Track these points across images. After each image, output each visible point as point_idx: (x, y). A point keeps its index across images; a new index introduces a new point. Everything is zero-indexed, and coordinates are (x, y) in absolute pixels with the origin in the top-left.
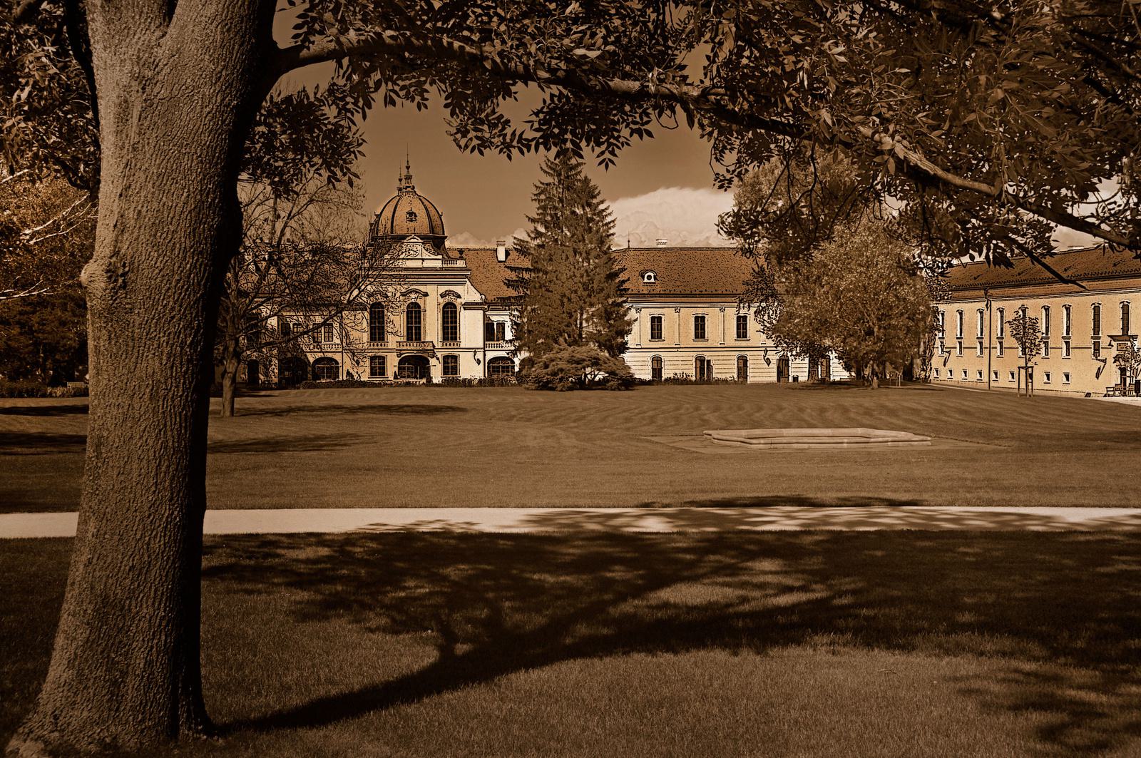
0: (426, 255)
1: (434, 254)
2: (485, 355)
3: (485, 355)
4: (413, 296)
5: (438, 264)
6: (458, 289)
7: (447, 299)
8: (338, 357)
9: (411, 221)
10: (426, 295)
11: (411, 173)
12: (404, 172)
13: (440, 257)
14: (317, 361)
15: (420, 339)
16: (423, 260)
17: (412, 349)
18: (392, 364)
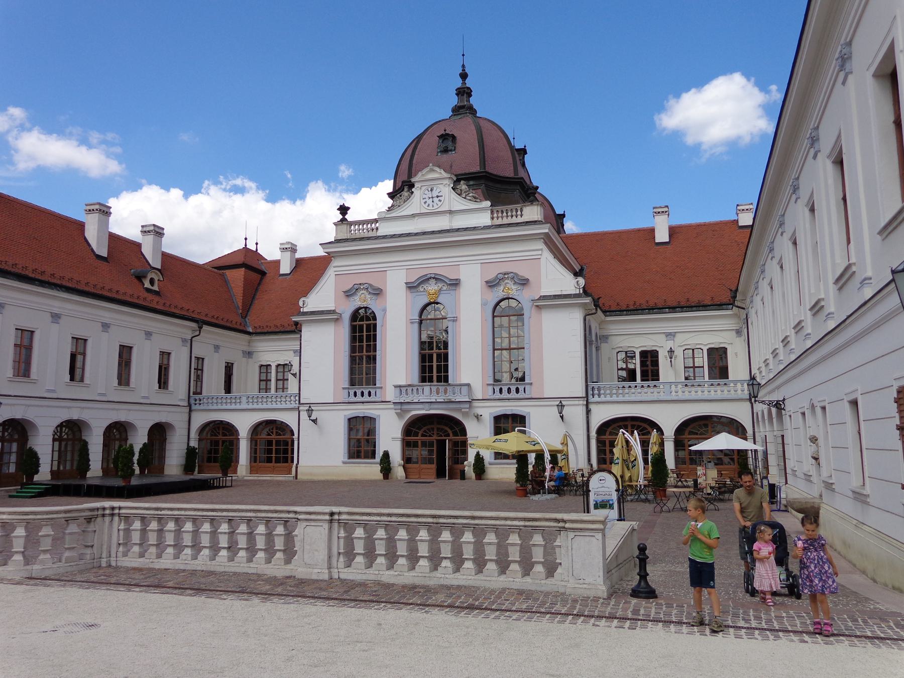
0: (458, 203)
1: (475, 199)
2: (588, 412)
3: (588, 412)
4: (432, 287)
5: (484, 219)
6: (523, 271)
7: (500, 293)
8: (289, 419)
9: (446, 151)
10: (455, 284)
11: (469, 83)
12: (459, 83)
13: (488, 203)
14: (257, 429)
15: (446, 380)
16: (451, 212)
17: (429, 400)
18: (389, 437)
